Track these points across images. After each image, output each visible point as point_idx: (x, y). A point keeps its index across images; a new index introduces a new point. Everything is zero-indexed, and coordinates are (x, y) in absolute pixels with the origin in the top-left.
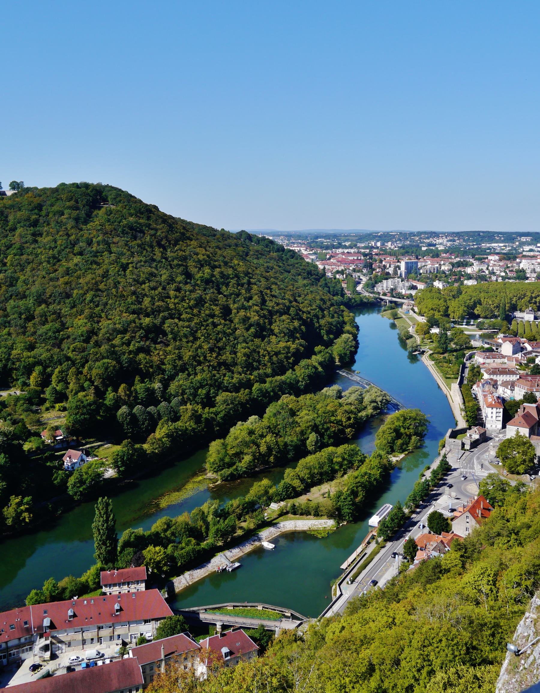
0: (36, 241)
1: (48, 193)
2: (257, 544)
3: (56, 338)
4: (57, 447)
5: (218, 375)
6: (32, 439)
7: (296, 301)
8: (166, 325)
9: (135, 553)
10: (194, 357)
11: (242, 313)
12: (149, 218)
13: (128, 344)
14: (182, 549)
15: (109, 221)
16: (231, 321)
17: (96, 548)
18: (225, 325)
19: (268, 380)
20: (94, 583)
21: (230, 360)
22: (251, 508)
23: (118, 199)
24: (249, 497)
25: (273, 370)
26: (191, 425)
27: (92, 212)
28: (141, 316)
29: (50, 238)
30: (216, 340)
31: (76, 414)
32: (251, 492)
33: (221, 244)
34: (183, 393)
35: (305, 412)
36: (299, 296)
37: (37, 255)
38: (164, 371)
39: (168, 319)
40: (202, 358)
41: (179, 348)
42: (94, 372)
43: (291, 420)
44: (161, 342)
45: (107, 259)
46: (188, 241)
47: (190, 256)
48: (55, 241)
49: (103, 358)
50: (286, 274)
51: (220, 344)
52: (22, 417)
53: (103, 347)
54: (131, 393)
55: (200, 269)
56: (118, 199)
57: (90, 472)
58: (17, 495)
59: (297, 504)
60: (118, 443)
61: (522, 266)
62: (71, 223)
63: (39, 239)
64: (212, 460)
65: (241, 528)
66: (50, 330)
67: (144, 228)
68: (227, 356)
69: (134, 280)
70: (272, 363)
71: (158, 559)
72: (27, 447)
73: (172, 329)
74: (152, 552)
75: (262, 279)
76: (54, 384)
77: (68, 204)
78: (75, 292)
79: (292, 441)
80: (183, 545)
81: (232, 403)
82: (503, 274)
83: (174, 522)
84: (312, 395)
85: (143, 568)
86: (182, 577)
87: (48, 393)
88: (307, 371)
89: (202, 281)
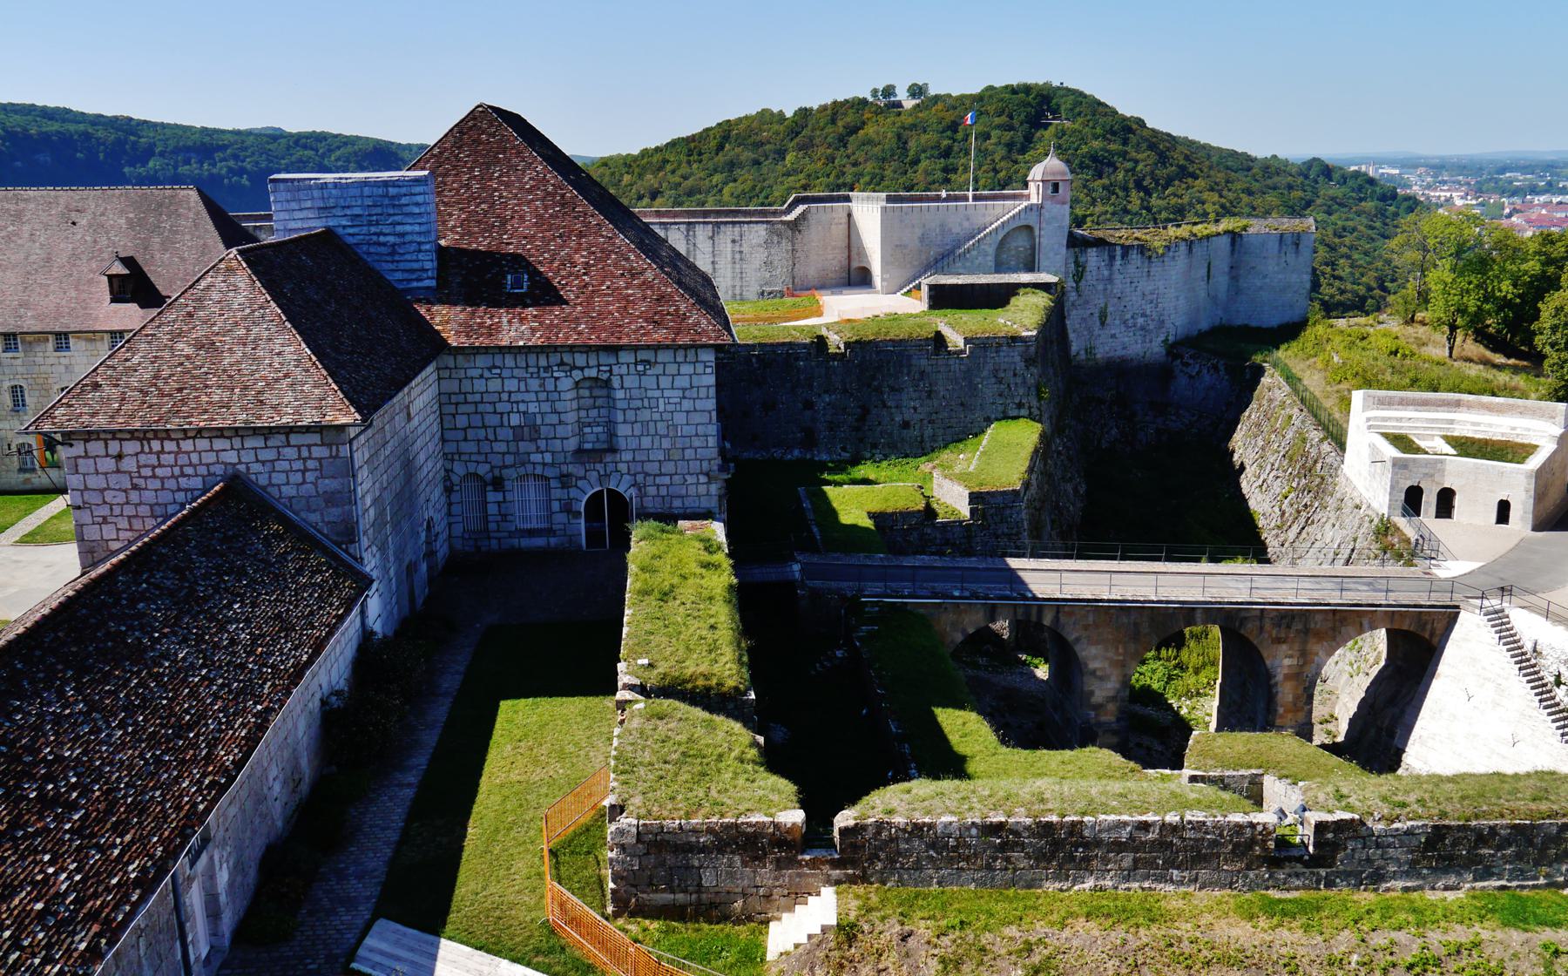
1: (968, 102)
12: (1125, 142)
36: (1393, 281)
47: (1191, 204)
62: (1001, 152)
63: (953, 177)
77: (997, 120)
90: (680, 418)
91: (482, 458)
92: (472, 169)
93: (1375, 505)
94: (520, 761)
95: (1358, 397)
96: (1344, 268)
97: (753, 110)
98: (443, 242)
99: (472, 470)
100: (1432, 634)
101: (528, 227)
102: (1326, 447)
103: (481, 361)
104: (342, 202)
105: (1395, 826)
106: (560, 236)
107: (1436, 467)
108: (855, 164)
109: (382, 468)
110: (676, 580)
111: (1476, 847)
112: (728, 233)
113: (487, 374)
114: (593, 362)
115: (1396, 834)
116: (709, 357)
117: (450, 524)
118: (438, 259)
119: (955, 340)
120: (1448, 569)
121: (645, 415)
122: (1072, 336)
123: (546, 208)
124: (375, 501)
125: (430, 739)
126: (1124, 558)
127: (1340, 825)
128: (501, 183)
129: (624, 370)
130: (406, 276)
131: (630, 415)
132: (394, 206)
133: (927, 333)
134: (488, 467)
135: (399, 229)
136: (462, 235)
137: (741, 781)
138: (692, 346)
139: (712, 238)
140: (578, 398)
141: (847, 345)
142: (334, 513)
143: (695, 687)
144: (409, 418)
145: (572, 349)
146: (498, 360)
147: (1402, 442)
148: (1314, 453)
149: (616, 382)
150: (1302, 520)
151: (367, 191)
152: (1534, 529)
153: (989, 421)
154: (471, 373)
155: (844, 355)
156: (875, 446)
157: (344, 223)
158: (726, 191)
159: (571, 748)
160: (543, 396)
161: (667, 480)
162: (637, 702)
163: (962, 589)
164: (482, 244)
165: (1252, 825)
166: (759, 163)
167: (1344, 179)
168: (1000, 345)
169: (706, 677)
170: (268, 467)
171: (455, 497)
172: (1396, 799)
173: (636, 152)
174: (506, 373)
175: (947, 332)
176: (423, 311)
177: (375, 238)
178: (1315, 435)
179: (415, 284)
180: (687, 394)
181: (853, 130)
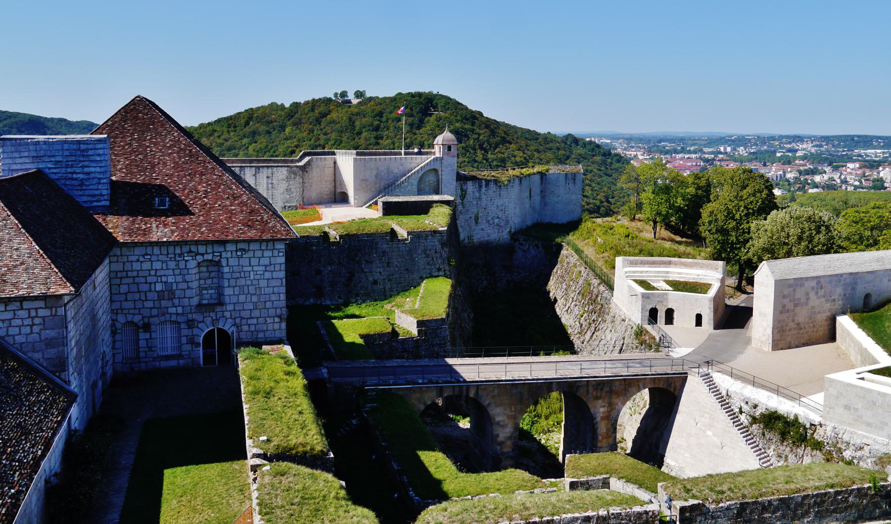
0: (378, 144)
1: (388, 101)
7: (609, 202)
15: (438, 126)
29: (389, 141)
33: (541, 148)
36: (613, 198)
47: (508, 157)
50: (605, 178)
61: (881, 175)
63: (381, 141)
82: (857, 183)
90: (263, 283)
91: (137, 311)
92: (132, 134)
93: (633, 319)
94: (184, 511)
95: (619, 260)
97: (266, 103)
98: (114, 178)
99: (129, 319)
100: (675, 389)
101: (168, 169)
102: (602, 288)
103: (138, 251)
104: (49, 153)
105: (721, 505)
106: (189, 175)
107: (664, 297)
108: (325, 134)
109: (81, 321)
110: (272, 384)
111: (762, 513)
112: (265, 173)
113: (141, 259)
114: (210, 250)
115: (721, 510)
116: (281, 246)
117: (114, 355)
118: (111, 188)
119: (402, 233)
120: (679, 352)
121: (242, 282)
122: (460, 230)
123: (180, 158)
124: (77, 343)
125: (119, 500)
126: (510, 355)
127: (693, 508)
128: (151, 143)
129: (229, 255)
130: (89, 199)
131: (233, 282)
132: (84, 156)
133: (386, 229)
134: (140, 317)
135: (86, 170)
136: (126, 174)
137: (341, 512)
138: (271, 240)
139: (255, 175)
140: (199, 272)
141: (341, 237)
142: (52, 353)
143: (297, 452)
144: (95, 288)
145: (197, 243)
146: (149, 251)
147: (643, 284)
148: (595, 291)
149: (224, 263)
150: (593, 329)
151: (66, 146)
152: (715, 329)
153: (422, 279)
154: (131, 258)
155: (339, 242)
156: (357, 295)
157: (50, 166)
158: (251, 148)
159: (216, 499)
160: (177, 272)
161: (255, 321)
162: (264, 465)
163: (423, 378)
164: (140, 179)
165: (646, 513)
167: (585, 144)
168: (427, 236)
169: (304, 445)
170: (7, 324)
171: (118, 337)
172: (717, 489)
173: (196, 125)
174: (154, 258)
175: (397, 229)
176: (100, 220)
177: (70, 175)
178: (596, 282)
179: (95, 204)
180: (268, 268)
181: (324, 115)
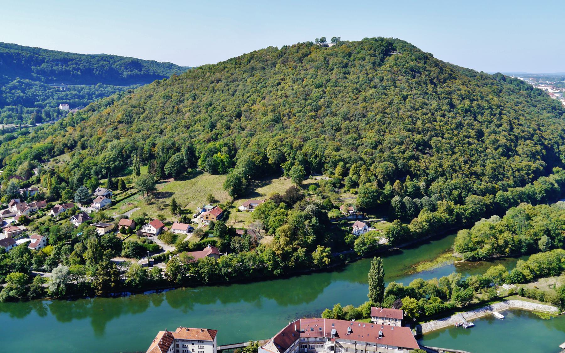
0: (346, 78)
1: (356, 45)
2: (489, 312)
3: (354, 144)
4: (349, 217)
5: (469, 182)
6: (334, 210)
7: (539, 129)
8: (432, 141)
9: (396, 299)
10: (451, 166)
11: (493, 136)
12: (425, 63)
13: (404, 153)
14: (430, 303)
15: (396, 64)
16: (483, 142)
17: (370, 291)
18: (478, 144)
19: (510, 189)
20: (366, 313)
21: (479, 171)
22: (486, 284)
23: (403, 49)
24: (486, 276)
25: (515, 182)
26: (445, 216)
27: (384, 58)
28: (414, 133)
29: (355, 76)
30: (470, 155)
31: (364, 197)
32: (488, 272)
33: (479, 83)
34: (441, 192)
35: (539, 218)
36: (543, 126)
37: (346, 87)
38: (427, 174)
39: (434, 136)
40: (457, 168)
41: (441, 159)
42: (378, 170)
43: (526, 223)
44: (428, 153)
45: (393, 91)
46: (454, 80)
48: (358, 78)
49: (385, 161)
50: (533, 108)
51: (473, 159)
52: (328, 195)
53: (385, 153)
54: (403, 187)
55: (461, 101)
56: (403, 49)
57: (370, 238)
58: (321, 246)
59: (525, 289)
60: (391, 221)
62: (370, 66)
63: (348, 76)
64: (459, 244)
65: (477, 298)
66: (350, 138)
67: (421, 70)
68: (477, 168)
69: (411, 107)
70: (515, 177)
71: (412, 307)
72: (330, 215)
73: (437, 145)
74: (407, 301)
75: (511, 111)
76: (350, 175)
78: (369, 113)
79: (526, 239)
80: (431, 301)
81: (478, 204)
83: (425, 283)
84: (547, 206)
85: (400, 311)
86: (428, 323)
87: (346, 181)
88: (544, 186)
89: (462, 110)
96: (523, 121)
97: (266, 47)
108: (305, 70)
158: (249, 80)
166: (264, 68)
167: (511, 81)
173: (216, 63)
181: (307, 55)
